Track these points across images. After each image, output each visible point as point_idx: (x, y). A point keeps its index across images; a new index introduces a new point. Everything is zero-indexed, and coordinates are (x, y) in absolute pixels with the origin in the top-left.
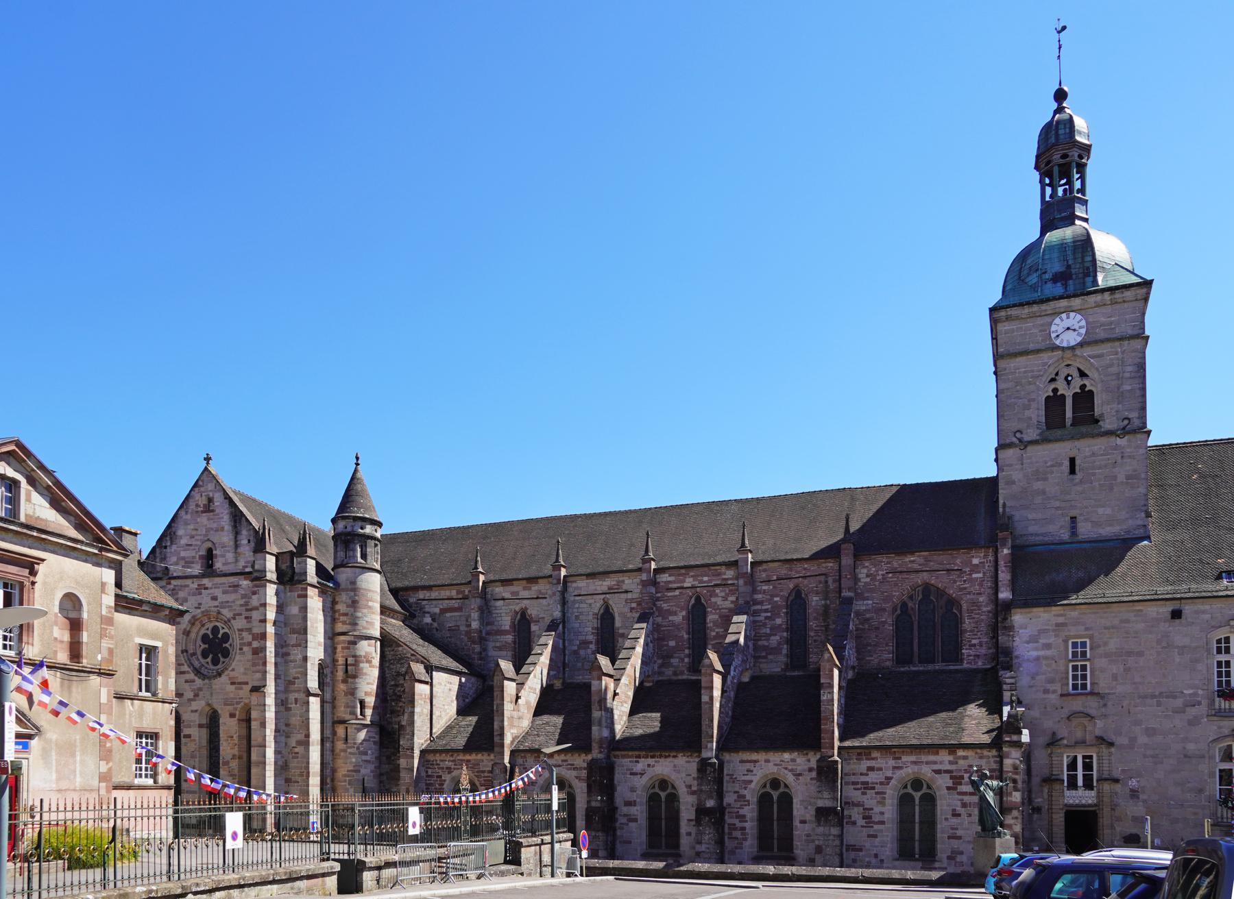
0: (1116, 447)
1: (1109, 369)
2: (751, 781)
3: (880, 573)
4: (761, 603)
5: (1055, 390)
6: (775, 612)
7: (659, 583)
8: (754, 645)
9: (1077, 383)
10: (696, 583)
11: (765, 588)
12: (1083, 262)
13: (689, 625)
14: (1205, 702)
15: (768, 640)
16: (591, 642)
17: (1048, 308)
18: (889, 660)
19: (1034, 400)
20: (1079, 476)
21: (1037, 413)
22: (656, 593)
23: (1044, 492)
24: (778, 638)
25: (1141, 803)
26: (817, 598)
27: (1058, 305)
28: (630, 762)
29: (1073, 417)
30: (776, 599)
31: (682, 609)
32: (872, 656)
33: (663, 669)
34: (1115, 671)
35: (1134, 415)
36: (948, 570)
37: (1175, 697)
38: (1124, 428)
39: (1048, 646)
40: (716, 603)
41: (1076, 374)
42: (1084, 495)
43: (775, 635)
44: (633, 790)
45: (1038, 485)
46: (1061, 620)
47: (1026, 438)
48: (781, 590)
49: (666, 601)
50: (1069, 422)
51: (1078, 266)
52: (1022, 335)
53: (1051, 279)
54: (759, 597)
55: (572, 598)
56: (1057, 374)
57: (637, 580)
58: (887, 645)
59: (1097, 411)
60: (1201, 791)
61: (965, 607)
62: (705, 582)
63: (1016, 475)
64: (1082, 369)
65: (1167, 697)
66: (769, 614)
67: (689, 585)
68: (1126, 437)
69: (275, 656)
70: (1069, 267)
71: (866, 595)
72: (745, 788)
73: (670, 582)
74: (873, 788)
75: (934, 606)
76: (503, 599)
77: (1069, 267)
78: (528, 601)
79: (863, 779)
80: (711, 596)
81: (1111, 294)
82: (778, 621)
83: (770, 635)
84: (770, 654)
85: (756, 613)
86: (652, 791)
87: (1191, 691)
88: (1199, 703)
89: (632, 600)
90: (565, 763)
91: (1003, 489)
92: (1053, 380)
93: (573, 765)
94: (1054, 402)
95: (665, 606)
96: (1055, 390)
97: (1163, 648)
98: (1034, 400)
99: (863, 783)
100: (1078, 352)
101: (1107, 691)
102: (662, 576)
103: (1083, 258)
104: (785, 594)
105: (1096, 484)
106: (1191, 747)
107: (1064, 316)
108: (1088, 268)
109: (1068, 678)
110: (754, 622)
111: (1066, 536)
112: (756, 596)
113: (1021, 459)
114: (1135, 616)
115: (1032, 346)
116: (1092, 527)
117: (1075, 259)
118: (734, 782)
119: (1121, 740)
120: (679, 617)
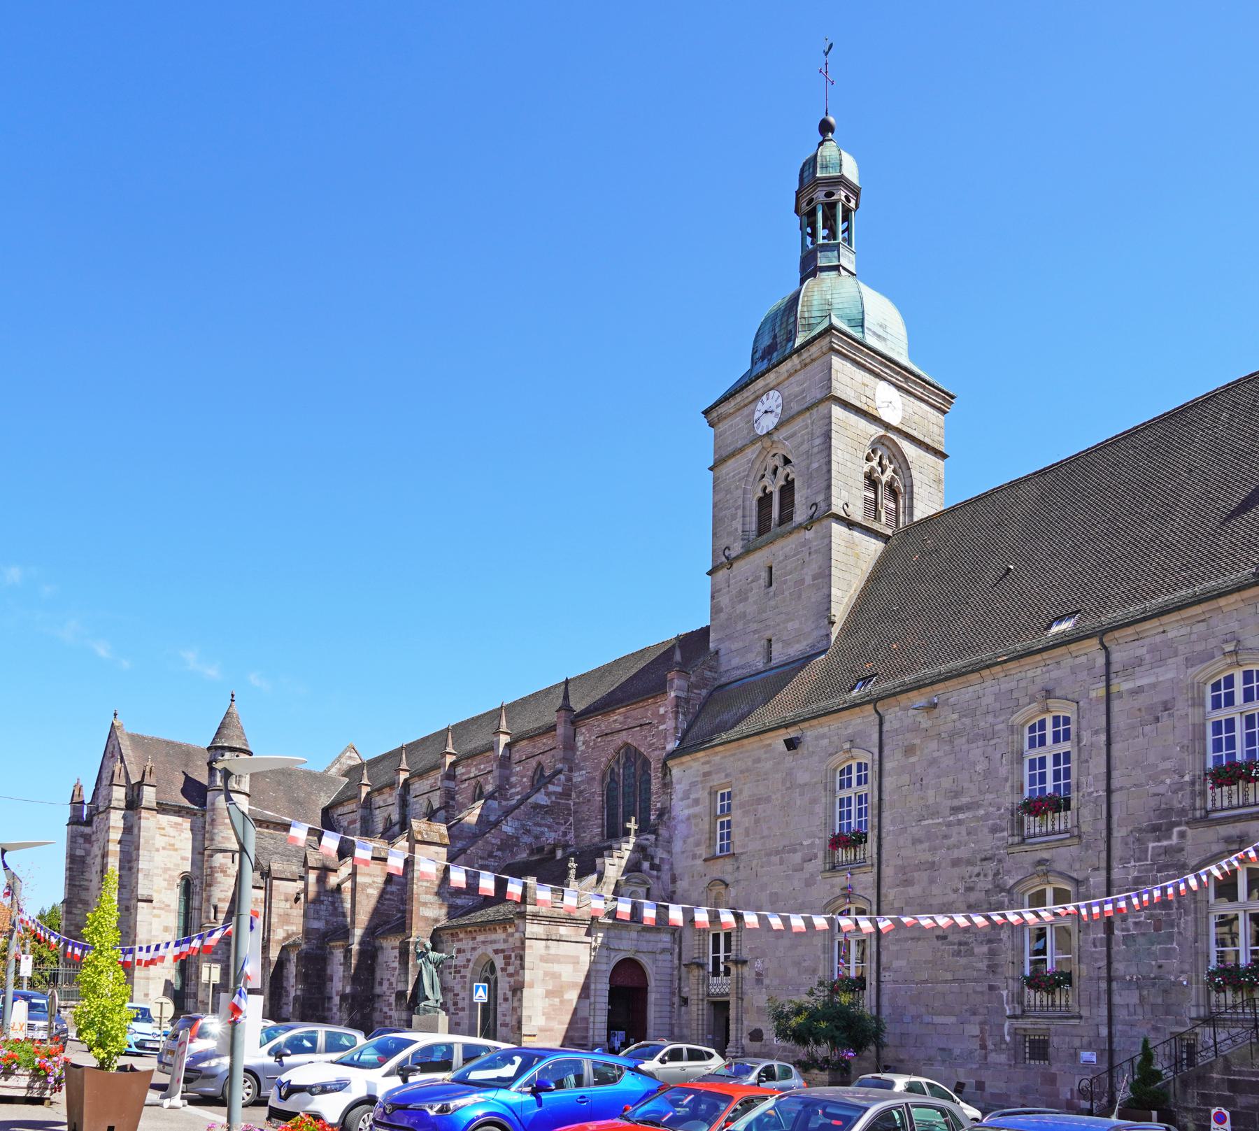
0: (805, 543)
23: (744, 615)
27: (757, 388)
35: (820, 498)
36: (641, 725)
38: (812, 517)
45: (740, 608)
46: (707, 768)
47: (733, 554)
69: (120, 870)
81: (799, 356)
100: (775, 437)
104: (530, 773)
105: (787, 593)
107: (764, 397)
113: (728, 581)
114: (766, 753)
115: (739, 444)
116: (783, 647)
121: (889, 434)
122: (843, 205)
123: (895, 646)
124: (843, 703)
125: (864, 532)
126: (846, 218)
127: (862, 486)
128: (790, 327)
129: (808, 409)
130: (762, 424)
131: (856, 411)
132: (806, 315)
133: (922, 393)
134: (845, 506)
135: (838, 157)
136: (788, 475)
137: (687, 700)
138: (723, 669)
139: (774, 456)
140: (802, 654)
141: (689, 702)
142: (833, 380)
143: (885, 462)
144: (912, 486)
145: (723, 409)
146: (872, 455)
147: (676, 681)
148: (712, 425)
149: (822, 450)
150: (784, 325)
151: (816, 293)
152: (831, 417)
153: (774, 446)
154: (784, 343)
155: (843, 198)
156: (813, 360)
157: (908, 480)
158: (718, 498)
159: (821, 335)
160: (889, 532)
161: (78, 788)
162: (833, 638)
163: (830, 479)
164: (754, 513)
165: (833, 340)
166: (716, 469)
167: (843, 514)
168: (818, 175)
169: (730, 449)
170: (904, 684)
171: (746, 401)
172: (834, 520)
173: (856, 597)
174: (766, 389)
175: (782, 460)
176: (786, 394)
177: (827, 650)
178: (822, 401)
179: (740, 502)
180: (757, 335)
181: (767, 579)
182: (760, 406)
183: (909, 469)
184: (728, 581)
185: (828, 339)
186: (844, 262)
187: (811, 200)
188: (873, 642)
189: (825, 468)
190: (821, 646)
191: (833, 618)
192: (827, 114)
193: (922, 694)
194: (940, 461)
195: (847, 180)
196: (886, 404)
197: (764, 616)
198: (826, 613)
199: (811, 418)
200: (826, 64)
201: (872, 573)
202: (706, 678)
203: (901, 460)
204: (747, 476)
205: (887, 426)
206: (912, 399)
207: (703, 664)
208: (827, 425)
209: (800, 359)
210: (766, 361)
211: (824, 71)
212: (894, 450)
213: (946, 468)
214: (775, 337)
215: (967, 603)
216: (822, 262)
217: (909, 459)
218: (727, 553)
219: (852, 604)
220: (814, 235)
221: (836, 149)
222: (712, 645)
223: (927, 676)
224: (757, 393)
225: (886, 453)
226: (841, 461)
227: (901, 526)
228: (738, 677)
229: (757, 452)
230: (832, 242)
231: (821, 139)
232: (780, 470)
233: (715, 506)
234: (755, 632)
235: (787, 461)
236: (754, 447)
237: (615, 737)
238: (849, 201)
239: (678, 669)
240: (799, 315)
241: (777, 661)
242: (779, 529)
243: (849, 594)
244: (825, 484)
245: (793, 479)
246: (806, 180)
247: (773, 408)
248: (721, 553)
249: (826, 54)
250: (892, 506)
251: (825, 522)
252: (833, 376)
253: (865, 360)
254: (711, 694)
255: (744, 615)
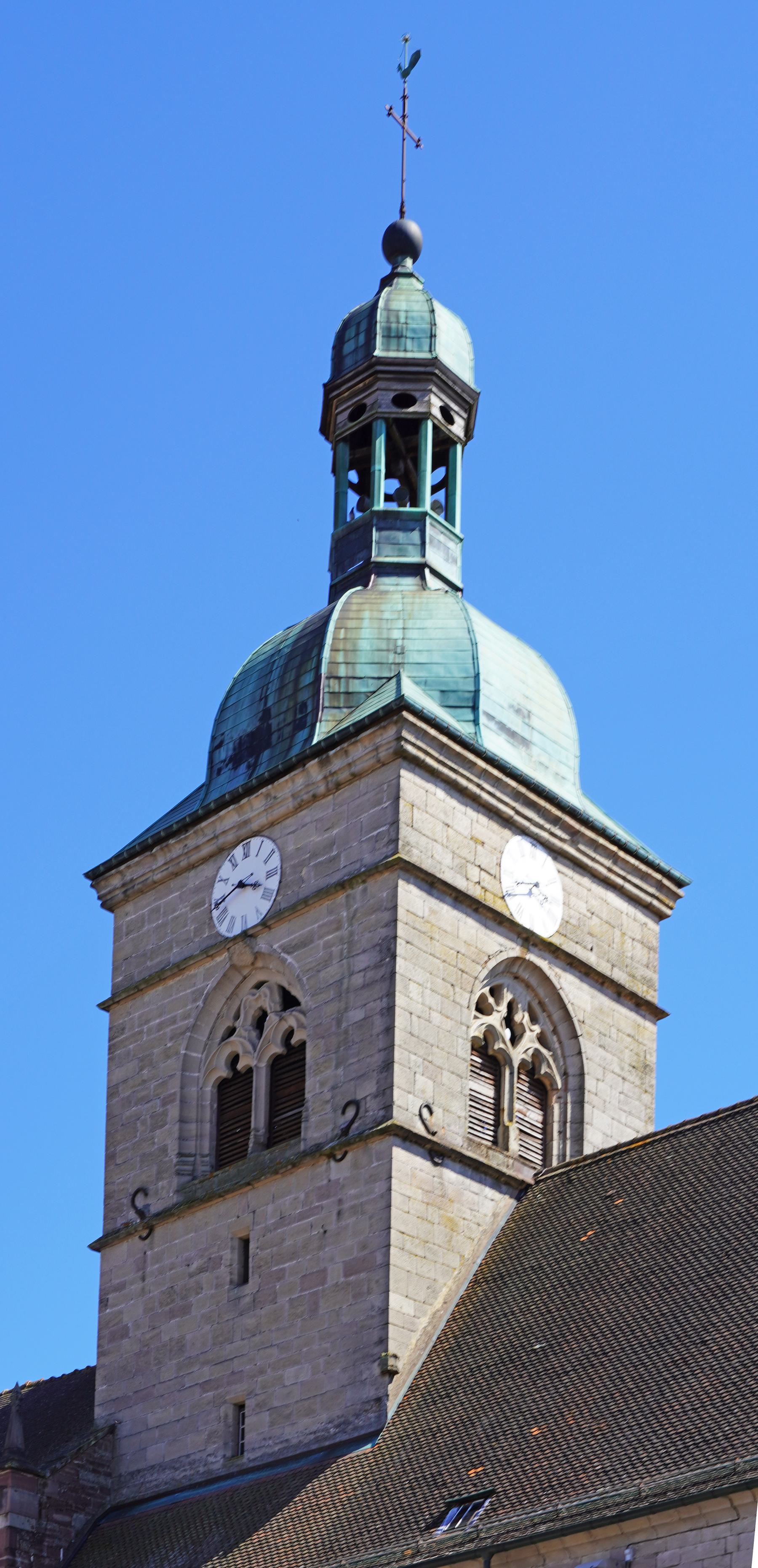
0: (330, 1189)
1: (322, 974)
17: (201, 840)
20: (250, 1288)
23: (180, 1346)
27: (220, 828)
38: (346, 1131)
42: (257, 1339)
45: (170, 1329)
47: (156, 1207)
52: (158, 927)
68: (349, 1157)
100: (262, 944)
105: (283, 1300)
107: (238, 851)
113: (142, 1265)
115: (175, 954)
116: (272, 1424)
121: (531, 957)
122: (435, 428)
123: (535, 1431)
124: (413, 1556)
125: (470, 1172)
126: (442, 458)
127: (464, 1068)
128: (304, 696)
129: (342, 885)
130: (231, 912)
131: (456, 899)
132: (342, 671)
133: (610, 870)
134: (425, 1112)
135: (427, 315)
136: (290, 1033)
137: (37, 1538)
138: (125, 1468)
139: (259, 986)
140: (317, 1440)
141: (40, 1542)
142: (402, 826)
143: (521, 1017)
144: (582, 1075)
145: (135, 870)
146: (491, 1000)
147: (9, 1492)
148: (108, 905)
149: (373, 982)
150: (289, 690)
151: (366, 623)
152: (395, 907)
153: (259, 964)
154: (287, 731)
155: (436, 412)
156: (355, 776)
157: (572, 1061)
158: (120, 1074)
159: (376, 720)
160: (527, 1175)
162: (392, 1408)
163: (390, 1048)
164: (209, 1114)
165: (405, 734)
166: (116, 1008)
167: (420, 1129)
168: (377, 353)
169: (153, 964)
170: (556, 1516)
171: (194, 857)
172: (398, 1140)
173: (447, 1316)
174: (244, 832)
175: (277, 998)
176: (291, 848)
177: (377, 1433)
178: (374, 870)
179: (174, 1087)
180: (223, 709)
181: (236, 1266)
182: (226, 870)
183: (575, 1036)
184: (142, 1265)
185: (391, 732)
186: (434, 557)
187: (359, 410)
188: (485, 1421)
189: (379, 1024)
190: (365, 1424)
191: (391, 1362)
192: (402, 213)
193: (595, 1542)
194: (648, 1024)
195: (445, 370)
196: (525, 889)
197: (228, 1350)
198: (376, 1350)
199: (348, 906)
200: (404, 97)
201: (485, 1264)
202: (84, 1488)
203: (557, 1015)
204: (194, 1028)
205: (527, 938)
206: (586, 881)
207: (77, 1455)
208: (386, 925)
209: (326, 771)
210: (243, 768)
211: (397, 114)
212: (541, 992)
213: (661, 1039)
214: (266, 714)
215: (704, 1343)
216: (381, 554)
217: (576, 1015)
218: (140, 1202)
219: (438, 1332)
220: (365, 488)
221: (422, 297)
222: (98, 1411)
223: (610, 1502)
224: (221, 840)
225: (525, 998)
226: (417, 1008)
227: (555, 1163)
228: (163, 1488)
229: (218, 976)
230: (408, 509)
231: (386, 269)
232: (272, 1019)
233: (112, 1092)
234: (205, 1386)
235: (289, 1001)
236: (210, 964)
238: (451, 421)
239: (15, 1464)
240: (324, 670)
241: (258, 1454)
242: (267, 1155)
243: (430, 1310)
244: (378, 1059)
245: (303, 1044)
246: (348, 362)
247: (260, 877)
248: (126, 1201)
249: (405, 74)
250: (535, 1116)
251: (377, 1145)
252: (404, 816)
253: (479, 786)
254: (94, 1526)
255: (180, 1346)
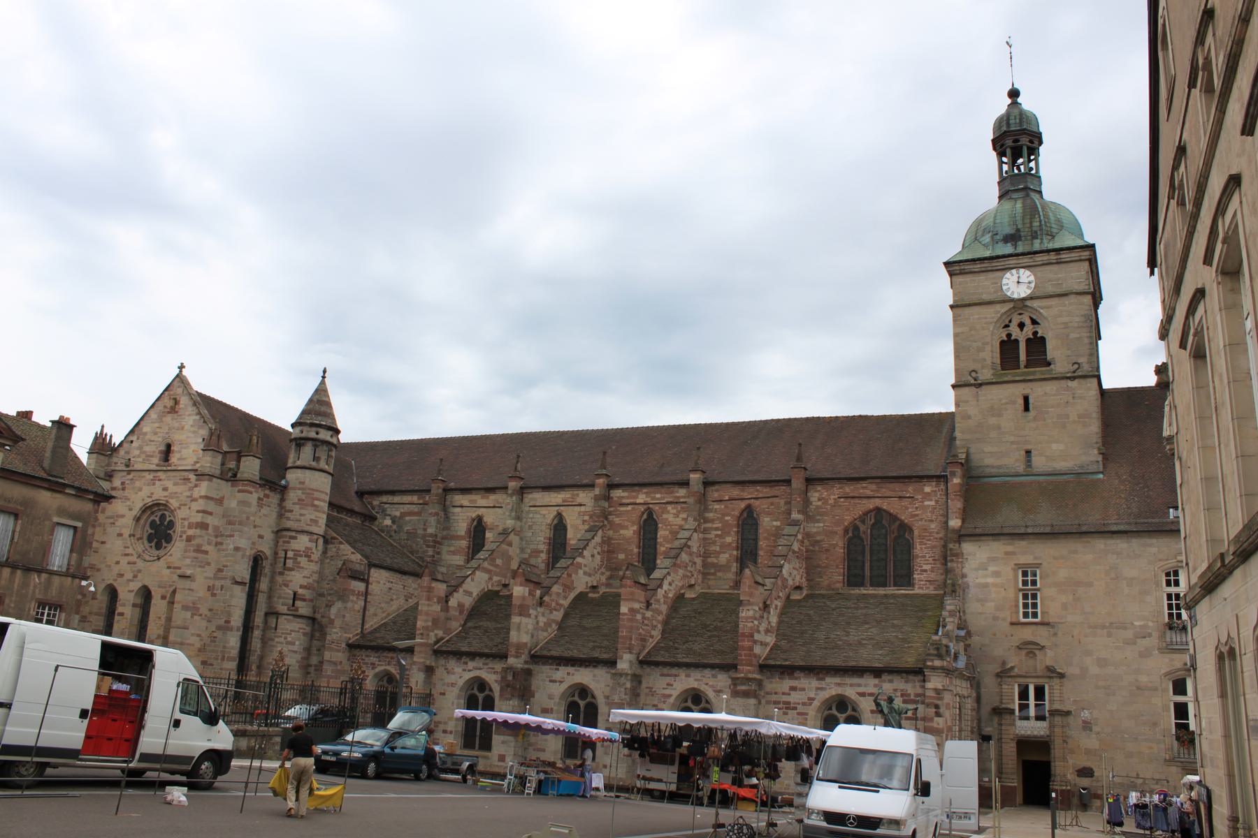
2: (670, 696)
3: (832, 497)
4: (712, 521)
5: (1009, 335)
6: (725, 531)
7: (612, 498)
8: (703, 561)
9: (1029, 329)
10: (649, 500)
11: (717, 507)
12: (1031, 226)
13: (640, 539)
14: (1155, 634)
15: (717, 557)
16: (542, 552)
18: (839, 582)
19: (987, 343)
20: (1032, 413)
21: (991, 354)
22: (609, 507)
23: (999, 428)
24: (727, 555)
25: (1094, 736)
26: (768, 519)
28: (550, 669)
29: (1027, 360)
30: (727, 518)
31: (633, 523)
32: (822, 577)
33: (611, 581)
34: (1065, 601)
37: (1125, 628)
38: (1074, 372)
39: (997, 574)
40: (667, 519)
41: (1028, 322)
43: (724, 553)
44: (551, 697)
45: (993, 421)
48: (733, 510)
49: (618, 516)
50: (1022, 364)
51: (1027, 230)
53: (1002, 240)
54: (710, 515)
55: (527, 509)
56: (1010, 321)
57: (591, 495)
58: (837, 567)
59: (1049, 357)
60: (1155, 724)
61: (916, 533)
62: (658, 499)
63: (972, 410)
64: (1034, 317)
65: (1118, 628)
66: (719, 533)
67: (642, 501)
70: (1018, 230)
71: (818, 517)
72: (664, 702)
73: (623, 497)
74: (795, 708)
75: (887, 531)
76: (462, 507)
77: (1018, 230)
78: (484, 510)
79: (785, 698)
80: (663, 513)
82: (729, 539)
83: (719, 553)
84: (719, 571)
85: (706, 531)
86: (570, 699)
87: (1142, 623)
88: (1150, 635)
89: (585, 513)
90: (486, 667)
91: (960, 423)
92: (1007, 326)
93: (493, 668)
94: (1008, 347)
95: (617, 520)
96: (1009, 335)
97: (1111, 579)
98: (987, 343)
99: (785, 703)
101: (1057, 620)
102: (616, 491)
103: (1031, 223)
106: (1144, 679)
108: (1036, 232)
109: (1017, 606)
110: (705, 539)
111: (1021, 468)
112: (707, 515)
117: (1024, 224)
118: (653, 695)
119: (1071, 671)
120: (630, 532)
158: (959, 330)
161: (97, 433)
237: (865, 501)
